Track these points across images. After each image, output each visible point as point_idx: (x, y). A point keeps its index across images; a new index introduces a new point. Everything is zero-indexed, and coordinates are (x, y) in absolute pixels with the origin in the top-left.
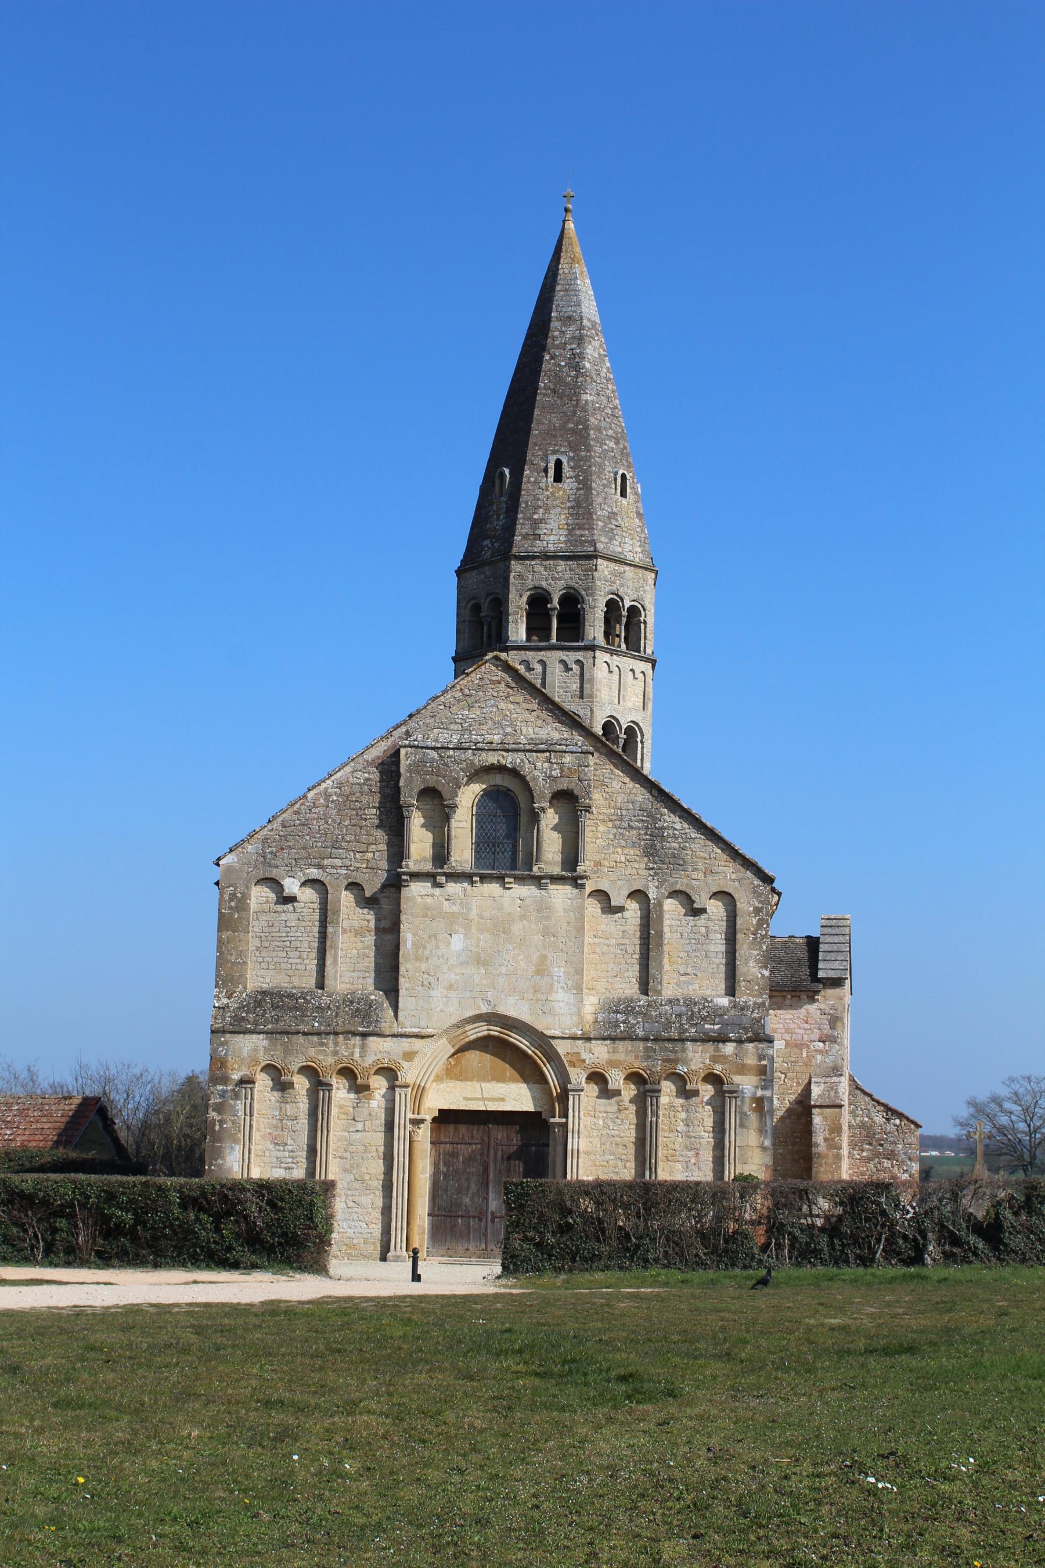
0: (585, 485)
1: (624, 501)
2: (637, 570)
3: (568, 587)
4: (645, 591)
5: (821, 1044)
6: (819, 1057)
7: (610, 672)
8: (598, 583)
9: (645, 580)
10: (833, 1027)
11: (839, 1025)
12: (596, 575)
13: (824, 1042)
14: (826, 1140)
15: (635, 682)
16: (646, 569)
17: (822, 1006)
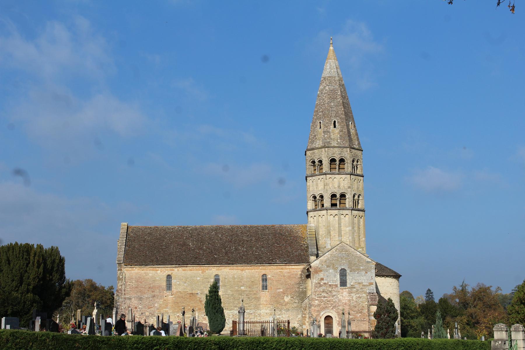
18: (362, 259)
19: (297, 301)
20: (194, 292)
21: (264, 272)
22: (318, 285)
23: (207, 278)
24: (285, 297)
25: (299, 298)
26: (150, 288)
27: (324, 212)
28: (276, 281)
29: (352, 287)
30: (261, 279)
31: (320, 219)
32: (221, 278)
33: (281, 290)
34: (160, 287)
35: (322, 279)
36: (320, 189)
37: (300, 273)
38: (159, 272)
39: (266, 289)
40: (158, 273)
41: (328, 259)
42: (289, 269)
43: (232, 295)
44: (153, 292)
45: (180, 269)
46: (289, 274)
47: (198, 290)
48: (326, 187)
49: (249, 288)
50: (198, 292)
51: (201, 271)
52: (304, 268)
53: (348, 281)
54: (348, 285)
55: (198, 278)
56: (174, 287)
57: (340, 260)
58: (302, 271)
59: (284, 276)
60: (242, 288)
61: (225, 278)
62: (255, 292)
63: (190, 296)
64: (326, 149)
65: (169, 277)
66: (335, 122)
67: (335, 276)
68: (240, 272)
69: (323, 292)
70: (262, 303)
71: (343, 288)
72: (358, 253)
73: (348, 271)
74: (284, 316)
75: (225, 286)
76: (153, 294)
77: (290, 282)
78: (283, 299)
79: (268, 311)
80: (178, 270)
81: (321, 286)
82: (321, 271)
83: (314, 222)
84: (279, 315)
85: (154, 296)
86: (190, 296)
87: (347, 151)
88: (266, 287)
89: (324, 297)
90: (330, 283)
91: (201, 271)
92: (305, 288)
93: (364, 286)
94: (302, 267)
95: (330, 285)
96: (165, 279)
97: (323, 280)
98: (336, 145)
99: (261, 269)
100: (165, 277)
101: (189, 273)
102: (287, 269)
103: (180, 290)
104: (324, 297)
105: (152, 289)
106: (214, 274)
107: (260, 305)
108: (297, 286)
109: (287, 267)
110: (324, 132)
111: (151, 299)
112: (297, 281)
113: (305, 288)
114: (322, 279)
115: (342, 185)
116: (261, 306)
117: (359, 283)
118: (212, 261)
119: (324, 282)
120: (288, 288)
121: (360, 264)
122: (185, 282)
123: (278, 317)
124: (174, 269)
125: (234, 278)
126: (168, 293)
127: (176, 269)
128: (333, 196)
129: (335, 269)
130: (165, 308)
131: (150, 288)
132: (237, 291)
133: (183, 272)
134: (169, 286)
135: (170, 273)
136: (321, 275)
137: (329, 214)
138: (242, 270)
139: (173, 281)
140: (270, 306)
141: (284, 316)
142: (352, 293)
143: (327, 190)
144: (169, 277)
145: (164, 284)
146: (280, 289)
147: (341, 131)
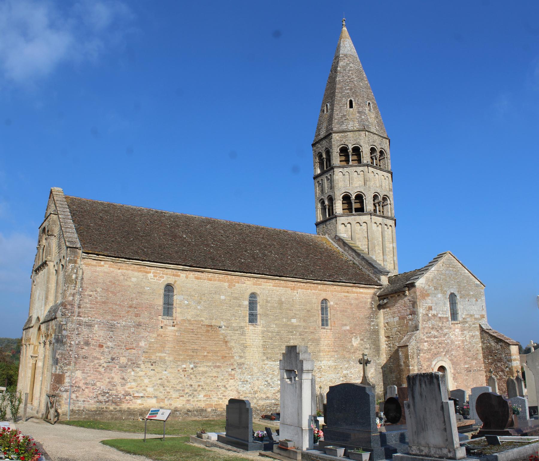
0: (332, 109)
1: (351, 109)
2: (354, 133)
3: (326, 148)
4: (360, 140)
5: (410, 316)
6: (410, 322)
7: (344, 175)
8: (333, 143)
9: (360, 135)
10: (414, 307)
11: (415, 305)
12: (332, 140)
13: (411, 315)
14: (404, 362)
15: (359, 176)
16: (359, 131)
17: (409, 298)
18: (471, 280)
19: (368, 346)
20: (214, 323)
21: (324, 295)
22: (426, 318)
23: (236, 298)
24: (353, 339)
25: (370, 341)
26: (131, 307)
27: (366, 218)
28: (341, 311)
29: (464, 322)
30: (320, 308)
31: (358, 227)
32: (259, 299)
33: (348, 328)
34: (151, 306)
35: (430, 308)
36: (356, 185)
37: (369, 300)
38: (151, 275)
39: (327, 325)
40: (148, 279)
41: (435, 277)
42: (357, 293)
43: (278, 333)
44: (137, 315)
45: (191, 275)
46: (357, 302)
47: (222, 319)
48: (368, 183)
49: (304, 321)
50: (222, 323)
51: (226, 284)
52: (375, 294)
53: (460, 312)
54: (460, 319)
55: (223, 297)
56: (179, 310)
57: (448, 279)
58: (373, 298)
59: (351, 304)
60: (294, 321)
61: (267, 302)
62: (312, 329)
63: (208, 331)
64: (367, 133)
65: (169, 288)
66: (369, 103)
67: (445, 304)
68: (289, 291)
69: (432, 328)
70: (322, 348)
71: (454, 322)
72: (467, 271)
73: (458, 297)
74: (353, 371)
75: (266, 315)
76: (137, 319)
77: (358, 314)
78: (351, 342)
79: (331, 363)
80: (187, 277)
81: (429, 319)
82: (428, 295)
83: (346, 231)
84: (347, 369)
85: (139, 325)
86: (208, 331)
87: (386, 144)
88: (327, 320)
89: (435, 337)
90: (439, 315)
91: (226, 284)
92: (377, 326)
93: (476, 319)
94: (372, 291)
95: (440, 318)
96: (162, 292)
97: (431, 310)
98: (375, 132)
99: (320, 290)
100: (163, 287)
101: (207, 283)
102: (354, 293)
103: (189, 318)
104: (435, 337)
105: (135, 309)
106: (249, 291)
107: (319, 351)
108: (368, 322)
109: (354, 289)
110: (359, 112)
111: (132, 330)
112: (366, 312)
113: (377, 326)
114: (430, 308)
115: (384, 185)
116: (321, 354)
117: (471, 316)
118: (245, 269)
119: (434, 312)
120: (356, 325)
121: (470, 288)
122: (199, 303)
123: (345, 372)
124: (179, 273)
125: (281, 303)
126: (166, 322)
127: (183, 275)
128: (375, 197)
129: (444, 293)
130: (161, 352)
131: (131, 307)
132: (286, 325)
133: (196, 281)
134: (168, 308)
135: (171, 280)
136: (429, 302)
137: (373, 221)
138: (293, 289)
139: (177, 299)
140: (333, 353)
141: (353, 371)
142: (464, 330)
143: (369, 187)
144: (169, 288)
145: (160, 302)
146: (346, 325)
147: (377, 117)
